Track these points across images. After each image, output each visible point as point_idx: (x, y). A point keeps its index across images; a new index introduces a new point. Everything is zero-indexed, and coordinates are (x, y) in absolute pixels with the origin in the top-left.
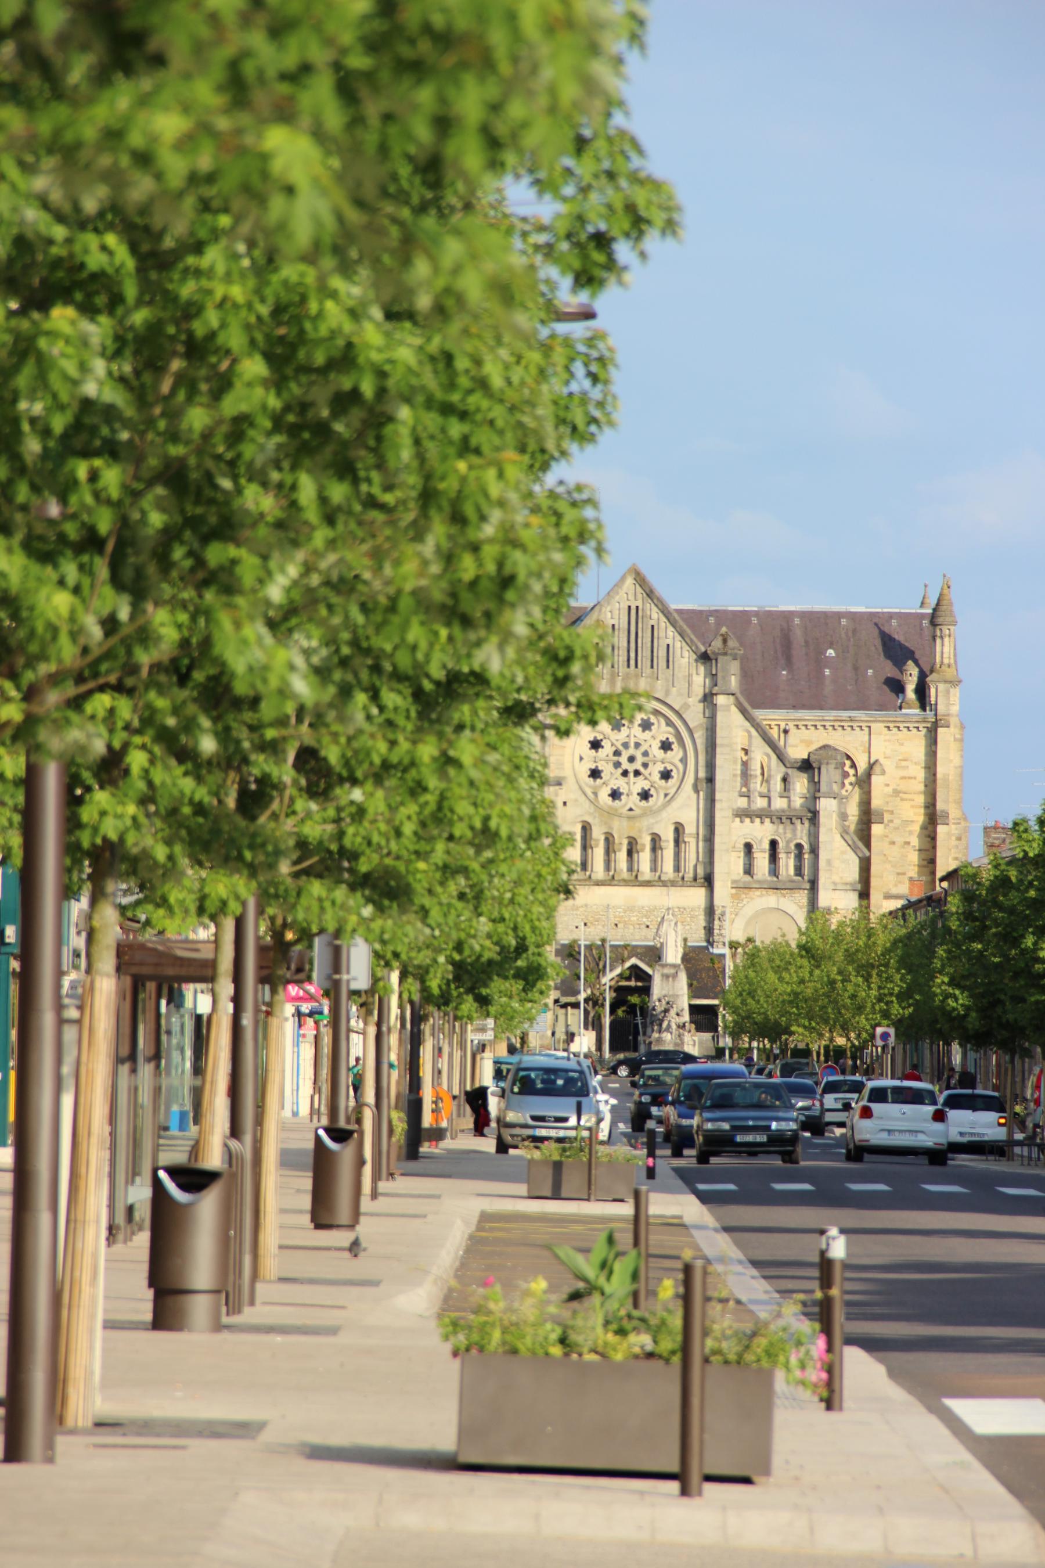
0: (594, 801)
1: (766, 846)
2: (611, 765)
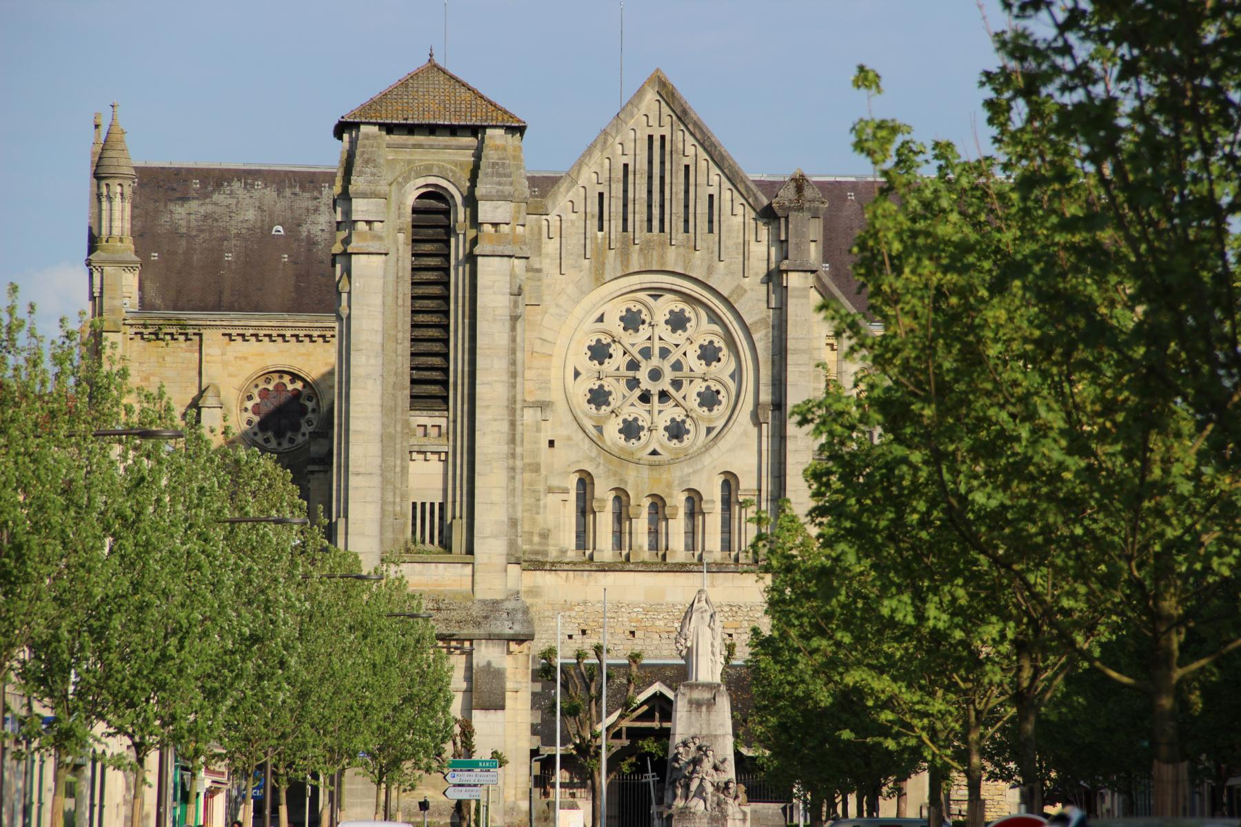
2: (623, 382)
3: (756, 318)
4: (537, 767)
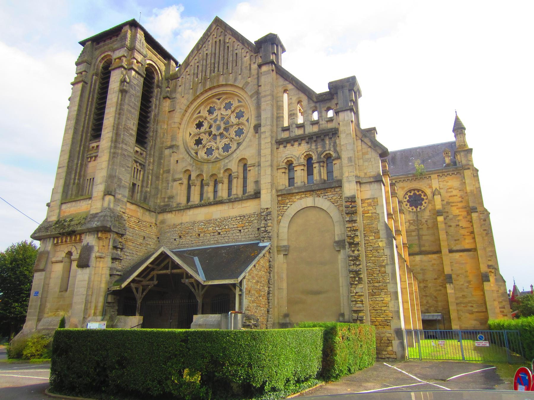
0: (195, 159)
1: (303, 161)
3: (253, 92)
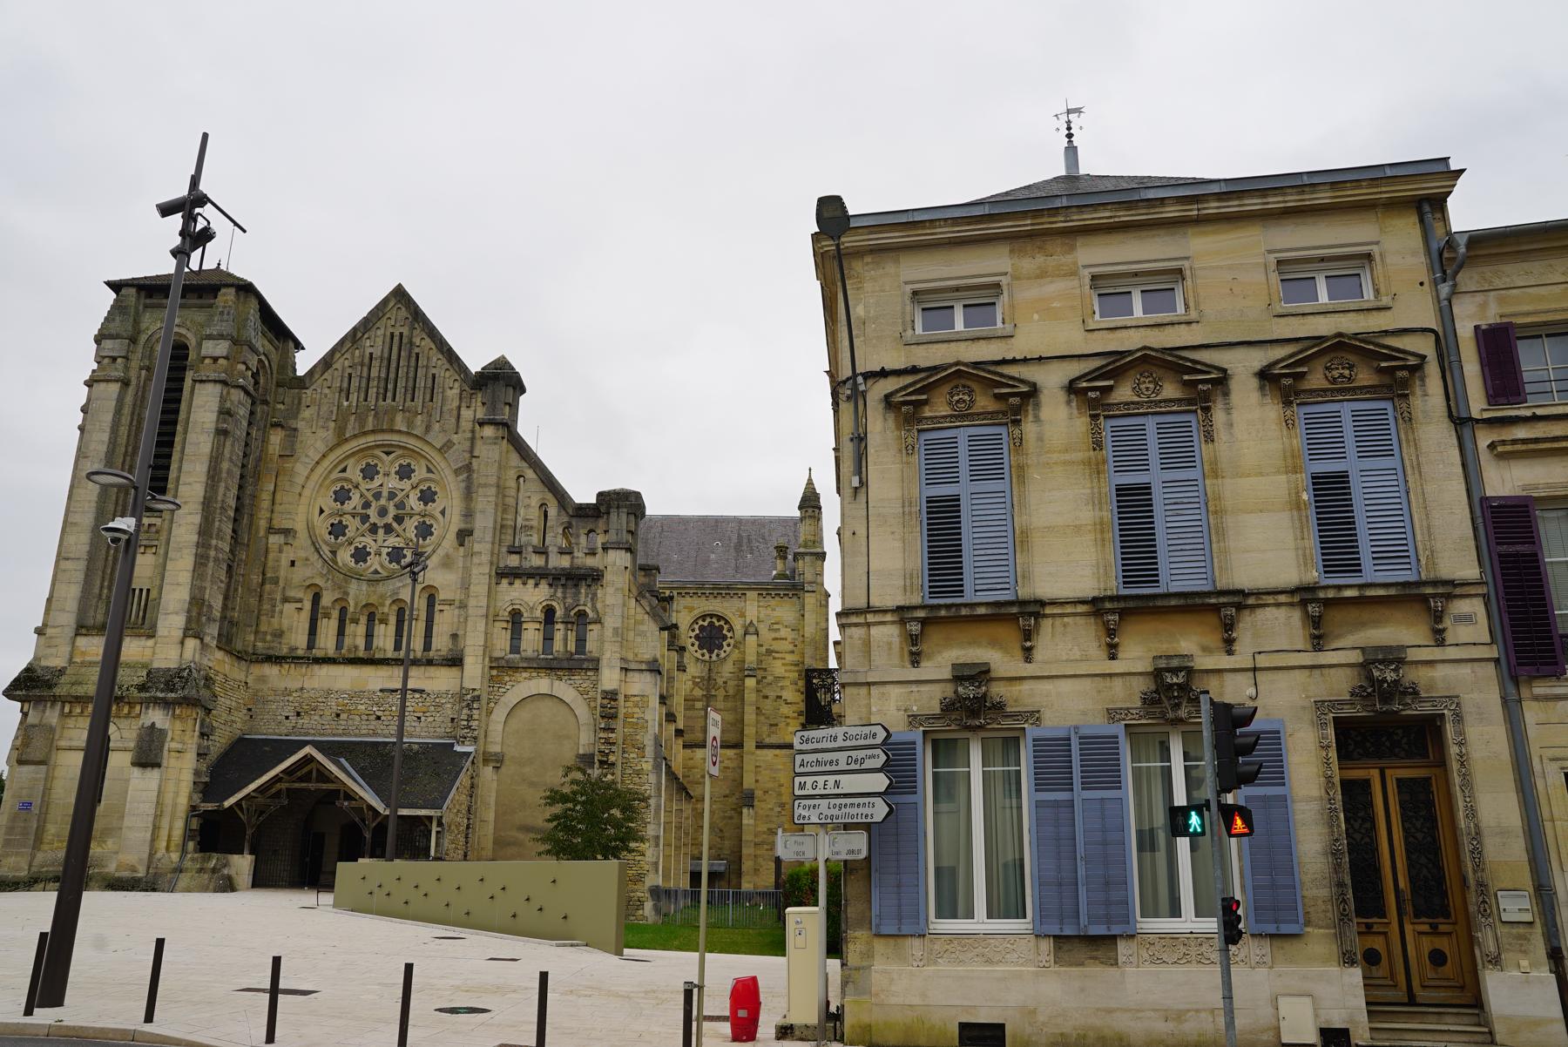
0: (331, 564)
1: (539, 614)
4: (195, 824)
